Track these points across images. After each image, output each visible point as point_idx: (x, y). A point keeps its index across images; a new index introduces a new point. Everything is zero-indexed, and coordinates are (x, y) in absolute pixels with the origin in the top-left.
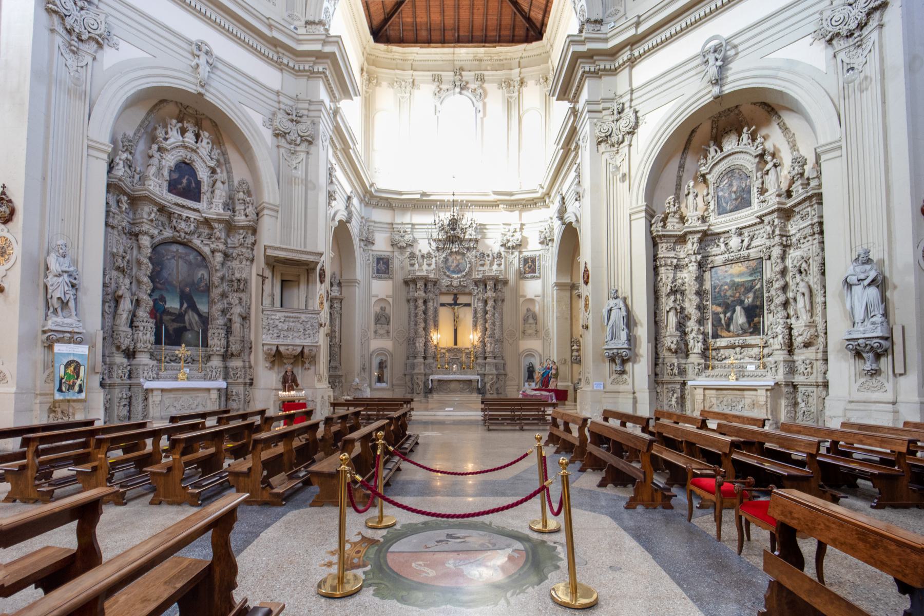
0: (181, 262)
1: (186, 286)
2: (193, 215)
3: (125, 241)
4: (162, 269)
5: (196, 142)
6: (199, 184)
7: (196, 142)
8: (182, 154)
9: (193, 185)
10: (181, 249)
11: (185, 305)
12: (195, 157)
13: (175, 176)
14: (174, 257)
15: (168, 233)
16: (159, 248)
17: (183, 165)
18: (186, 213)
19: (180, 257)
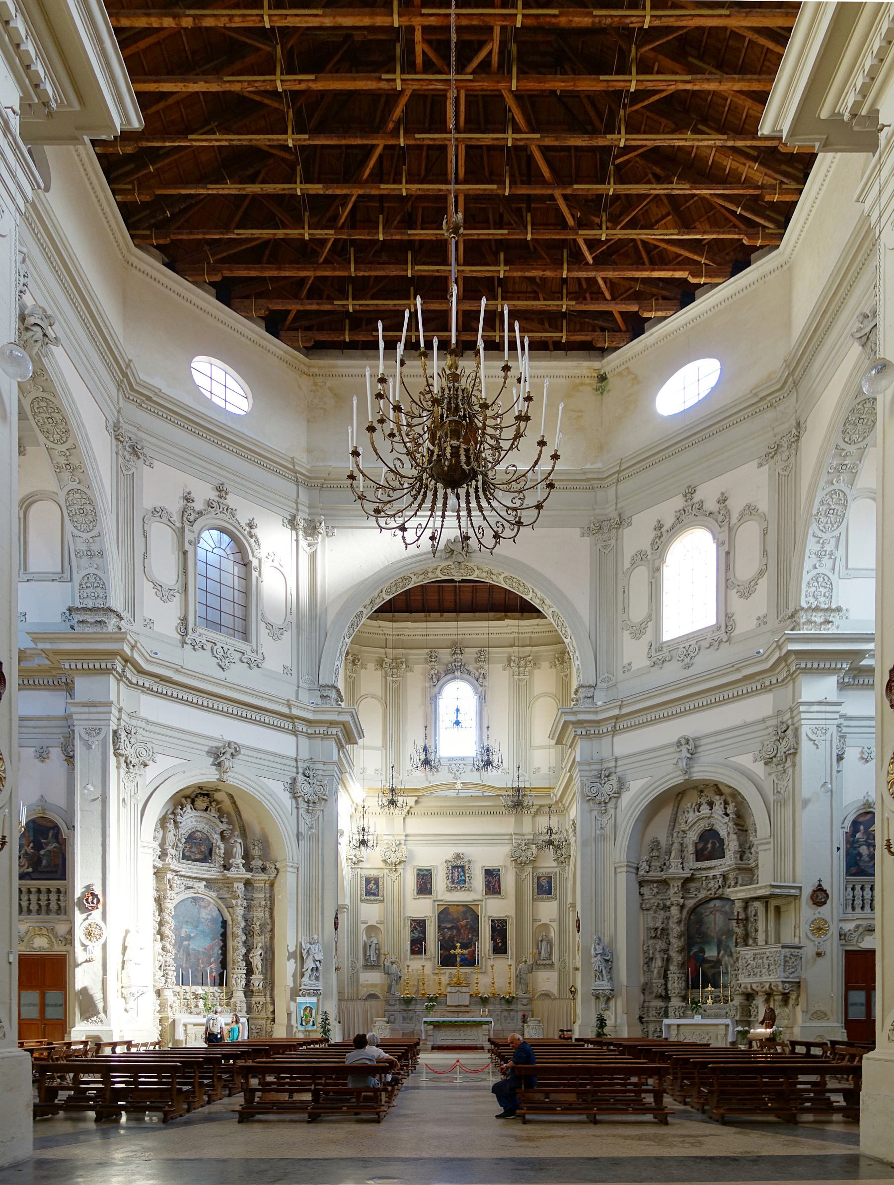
0: (718, 914)
1: (722, 935)
2: (716, 872)
3: (662, 914)
4: (701, 926)
5: (711, 810)
6: (722, 841)
7: (711, 810)
8: (702, 826)
9: (718, 845)
10: (718, 903)
11: (722, 952)
12: (713, 821)
13: (700, 846)
14: (711, 913)
15: (702, 895)
16: (698, 909)
17: (707, 833)
18: (711, 873)
19: (717, 911)
